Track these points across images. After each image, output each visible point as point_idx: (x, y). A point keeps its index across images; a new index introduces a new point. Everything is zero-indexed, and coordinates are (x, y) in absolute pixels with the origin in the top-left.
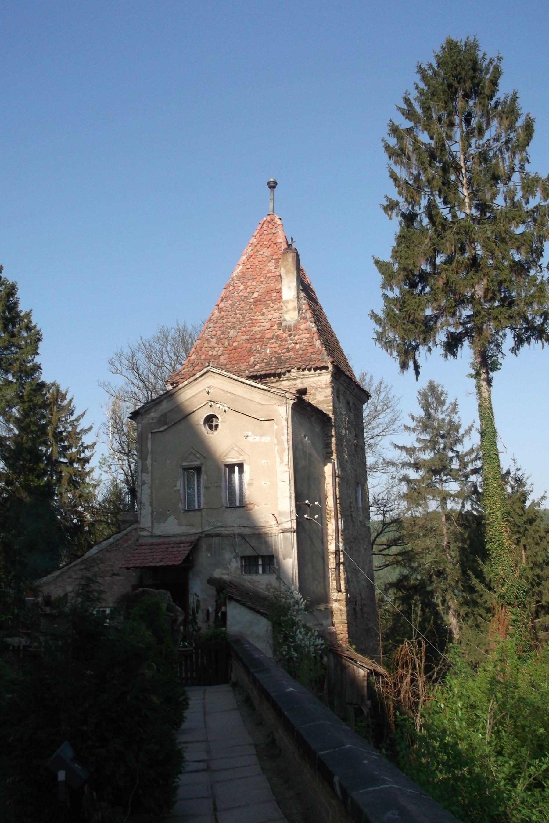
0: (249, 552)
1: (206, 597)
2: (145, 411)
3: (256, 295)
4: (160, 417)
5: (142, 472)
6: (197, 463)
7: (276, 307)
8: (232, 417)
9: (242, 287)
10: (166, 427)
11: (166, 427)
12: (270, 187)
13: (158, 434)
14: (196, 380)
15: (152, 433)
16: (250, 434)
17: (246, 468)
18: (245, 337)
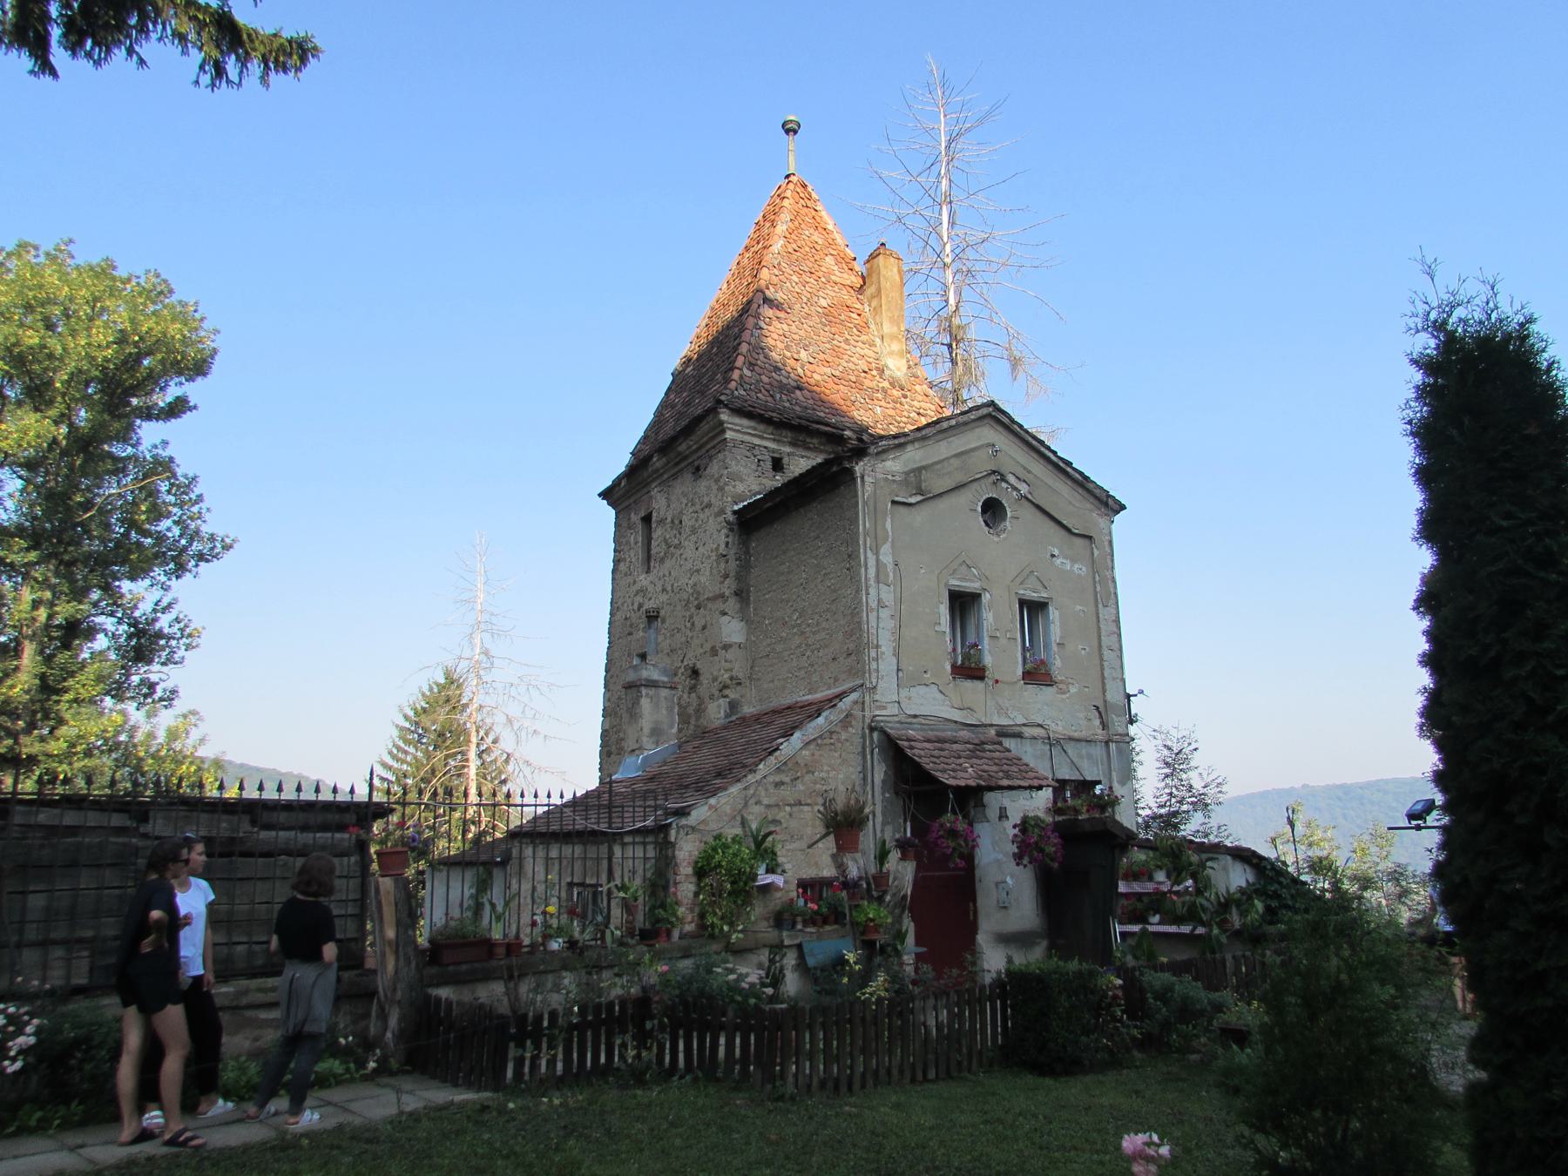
0: (1065, 773)
1: (1000, 856)
2: (878, 454)
3: (823, 303)
4: (907, 473)
5: (878, 581)
6: (971, 586)
7: (864, 338)
8: (1028, 513)
9: (795, 278)
10: (919, 498)
11: (919, 498)
12: (787, 132)
13: (902, 509)
14: (965, 424)
15: (894, 502)
16: (1056, 552)
17: (1054, 614)
18: (828, 371)
